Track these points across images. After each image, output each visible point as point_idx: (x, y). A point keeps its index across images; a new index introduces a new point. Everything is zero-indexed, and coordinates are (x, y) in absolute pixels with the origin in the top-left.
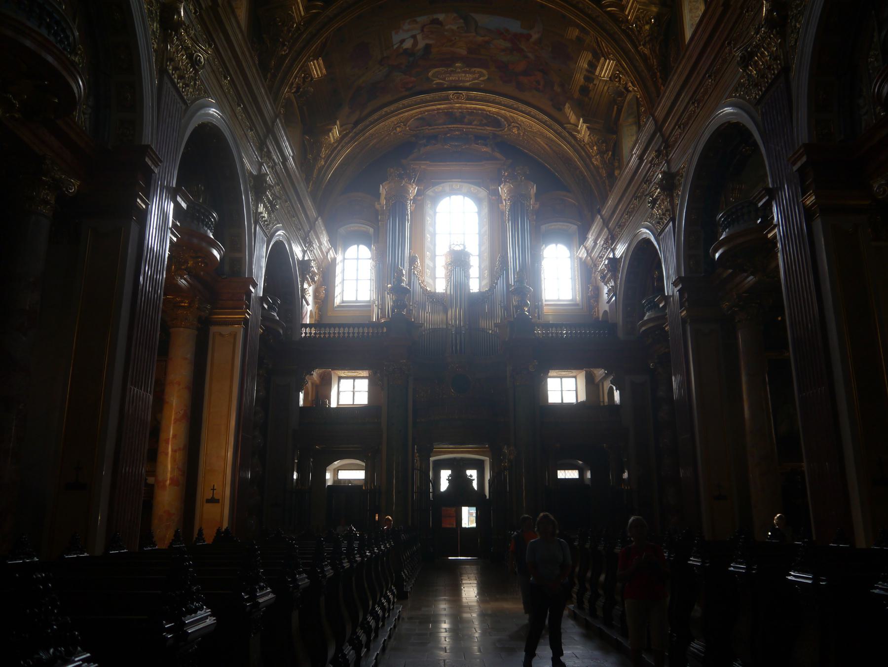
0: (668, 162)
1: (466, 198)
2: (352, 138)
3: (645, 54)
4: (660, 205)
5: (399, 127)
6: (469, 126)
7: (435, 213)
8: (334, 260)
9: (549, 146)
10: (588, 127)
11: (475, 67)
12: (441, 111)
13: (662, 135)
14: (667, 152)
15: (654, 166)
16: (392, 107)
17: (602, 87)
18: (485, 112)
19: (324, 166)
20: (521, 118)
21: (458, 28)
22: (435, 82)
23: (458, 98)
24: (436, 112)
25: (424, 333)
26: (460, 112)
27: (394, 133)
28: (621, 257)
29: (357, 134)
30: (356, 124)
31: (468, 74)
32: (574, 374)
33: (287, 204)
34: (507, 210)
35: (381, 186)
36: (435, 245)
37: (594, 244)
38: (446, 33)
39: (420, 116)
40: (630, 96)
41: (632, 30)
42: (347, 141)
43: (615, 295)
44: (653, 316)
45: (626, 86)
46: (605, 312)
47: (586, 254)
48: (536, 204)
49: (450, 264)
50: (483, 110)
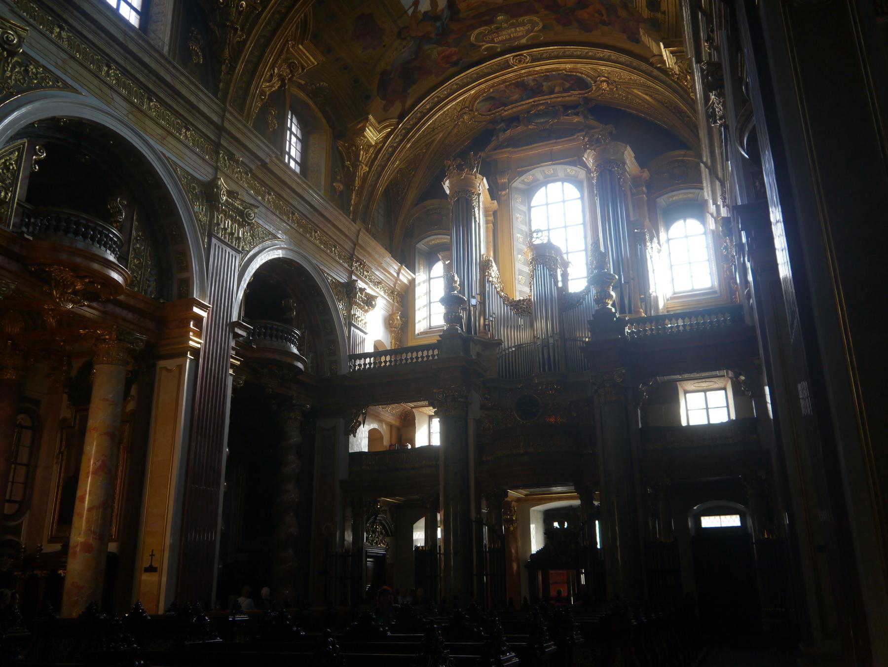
1: (565, 183)
5: (465, 113)
6: (552, 96)
7: (530, 208)
8: (412, 282)
9: (651, 96)
11: (521, 15)
18: (561, 72)
19: (369, 172)
22: (483, 47)
23: (520, 61)
25: (504, 353)
30: (401, 118)
31: (518, 27)
32: (721, 385)
39: (485, 95)
48: (644, 172)
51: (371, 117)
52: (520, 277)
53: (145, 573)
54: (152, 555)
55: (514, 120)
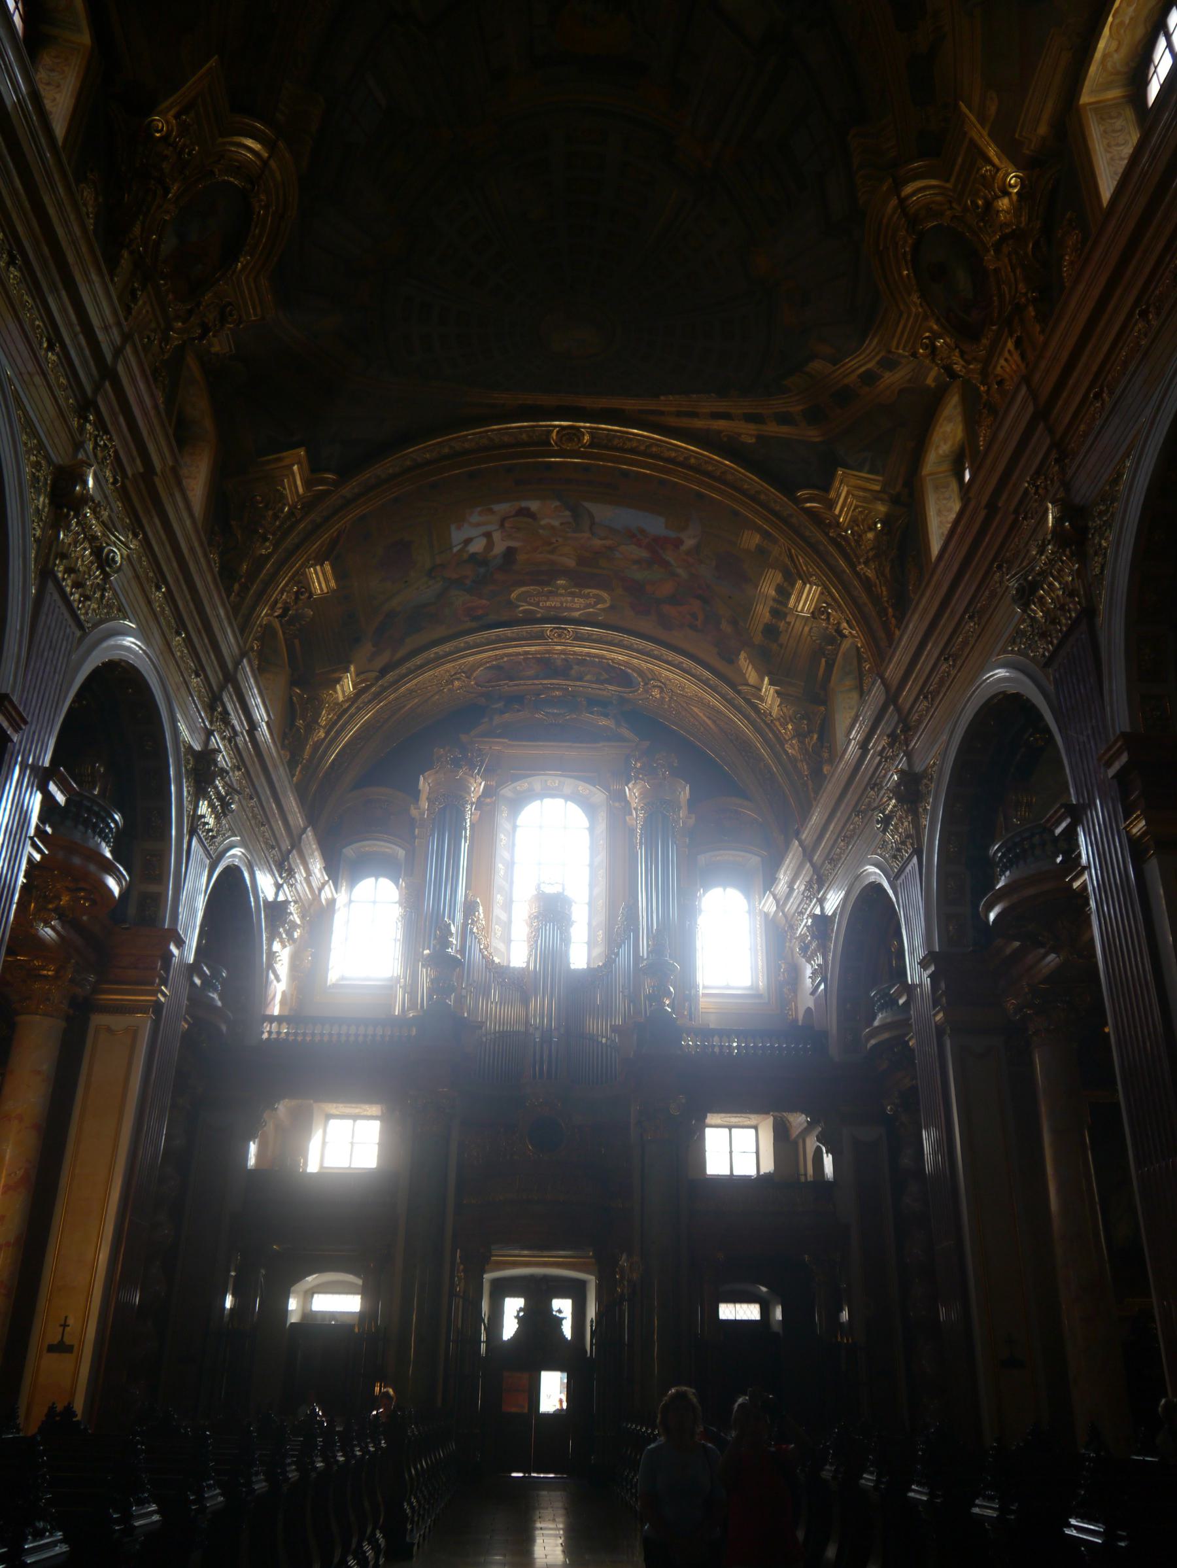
0: (909, 755)
1: (569, 803)
2: (377, 695)
3: (867, 578)
4: (896, 828)
5: (458, 679)
6: (578, 683)
7: (515, 827)
8: (332, 902)
9: (714, 722)
10: (777, 692)
12: (530, 656)
13: (898, 710)
14: (906, 739)
15: (886, 761)
16: (447, 647)
17: (800, 629)
20: (666, 673)
21: (562, 524)
22: (521, 609)
23: (560, 636)
24: (522, 657)
25: (484, 1039)
26: (563, 659)
27: (449, 690)
28: (834, 913)
29: (384, 689)
30: (383, 672)
31: (577, 597)
32: (753, 1122)
33: (252, 803)
34: (639, 826)
35: (421, 778)
36: (511, 883)
37: (788, 889)
38: (541, 531)
39: (494, 663)
40: (846, 644)
41: (845, 538)
42: (366, 700)
43: (824, 980)
44: (889, 1020)
45: (838, 627)
46: (809, 1010)
47: (775, 908)
49: (536, 917)
50: (602, 657)
51: (352, 668)
52: (497, 927)
53: (50, 1354)
54: (65, 1325)
55: (515, 700)
